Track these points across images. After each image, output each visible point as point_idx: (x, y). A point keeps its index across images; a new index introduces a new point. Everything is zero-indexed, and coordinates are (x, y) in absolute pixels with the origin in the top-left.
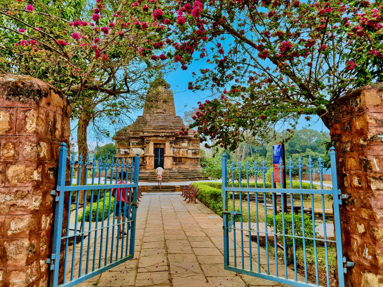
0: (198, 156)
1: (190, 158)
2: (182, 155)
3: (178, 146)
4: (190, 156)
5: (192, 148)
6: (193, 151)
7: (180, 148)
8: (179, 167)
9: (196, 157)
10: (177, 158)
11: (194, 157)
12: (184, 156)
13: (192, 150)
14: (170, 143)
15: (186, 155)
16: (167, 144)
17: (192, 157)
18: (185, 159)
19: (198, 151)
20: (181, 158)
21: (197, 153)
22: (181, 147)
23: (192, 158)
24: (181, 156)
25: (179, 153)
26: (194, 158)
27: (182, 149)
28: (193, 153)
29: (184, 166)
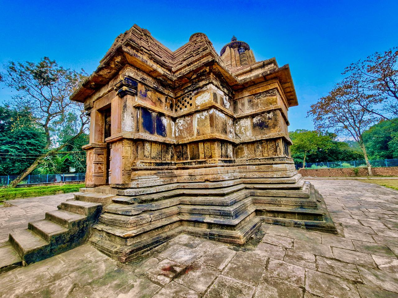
0: (272, 134)
1: (247, 144)
2: (198, 133)
3: (185, 111)
4: (249, 135)
5: (248, 111)
6: (255, 120)
7: (190, 115)
8: (191, 175)
9: (265, 137)
10: (185, 145)
11: (259, 138)
12: (201, 138)
13: (253, 116)
14: (122, 94)
15: (209, 133)
16: (115, 102)
17: (254, 139)
18: (207, 145)
19: (271, 115)
20: (196, 143)
21: (271, 123)
22: (193, 109)
23: (253, 143)
24: (195, 138)
25: (189, 128)
26: (260, 142)
27: (198, 115)
28: (254, 126)
29: (203, 171)
